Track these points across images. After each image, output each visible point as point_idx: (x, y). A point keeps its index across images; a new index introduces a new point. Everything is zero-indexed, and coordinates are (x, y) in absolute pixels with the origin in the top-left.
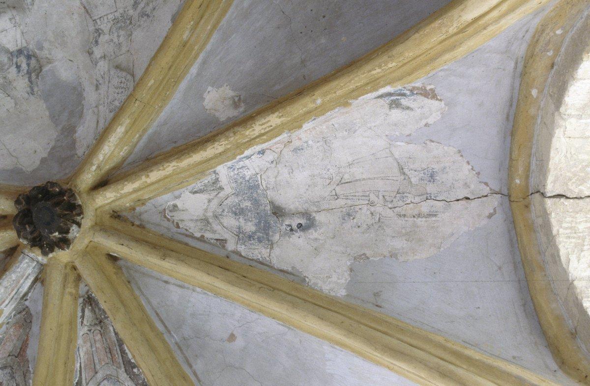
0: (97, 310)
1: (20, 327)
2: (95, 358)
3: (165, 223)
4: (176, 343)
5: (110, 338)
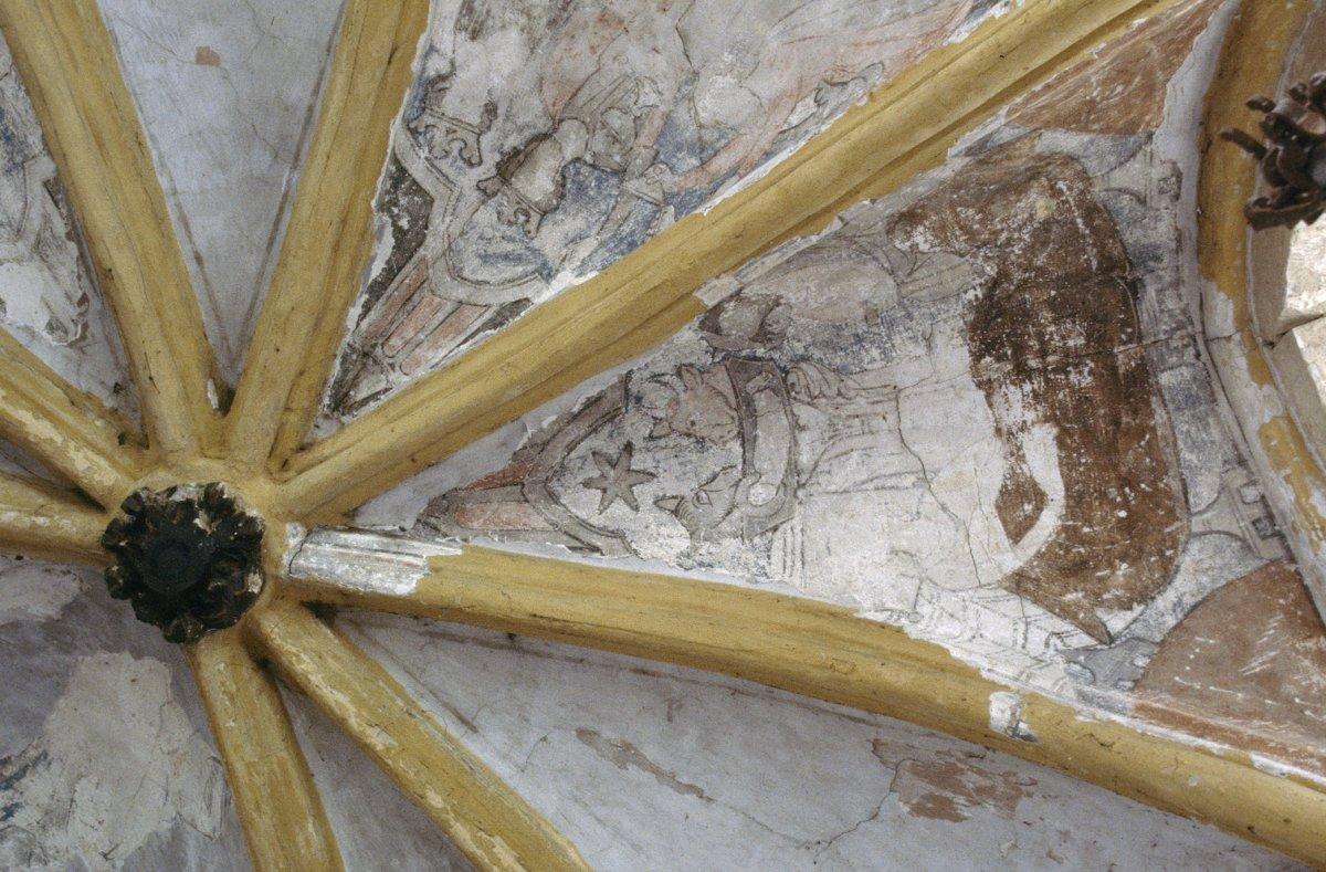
0: (350, 376)
1: (463, 512)
2: (437, 324)
3: (95, 329)
4: (294, 167)
5: (384, 316)
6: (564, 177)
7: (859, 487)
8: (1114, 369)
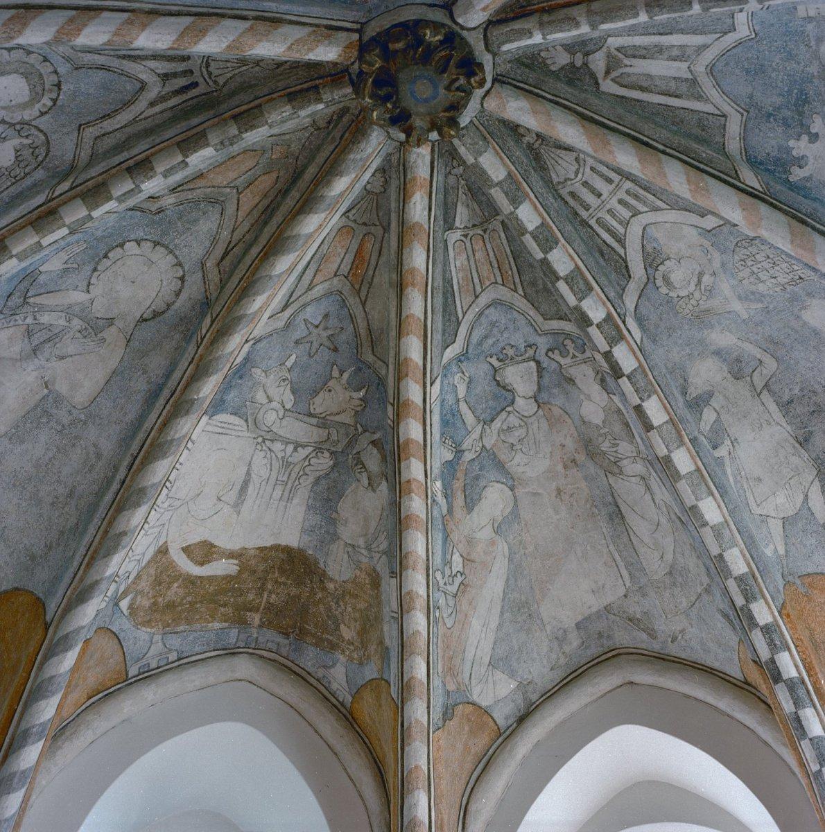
6: (509, 391)
7: (248, 474)
8: (250, 610)
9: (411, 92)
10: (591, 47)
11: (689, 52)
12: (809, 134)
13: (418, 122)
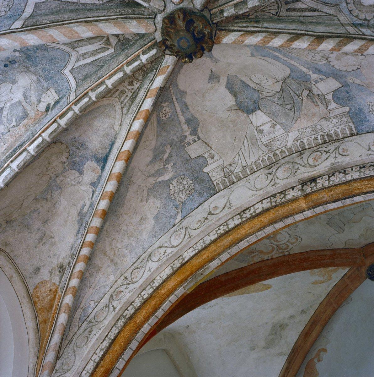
9: (188, 41)
10: (119, 44)
11: (82, 58)
12: (18, 51)
13: (180, 23)
